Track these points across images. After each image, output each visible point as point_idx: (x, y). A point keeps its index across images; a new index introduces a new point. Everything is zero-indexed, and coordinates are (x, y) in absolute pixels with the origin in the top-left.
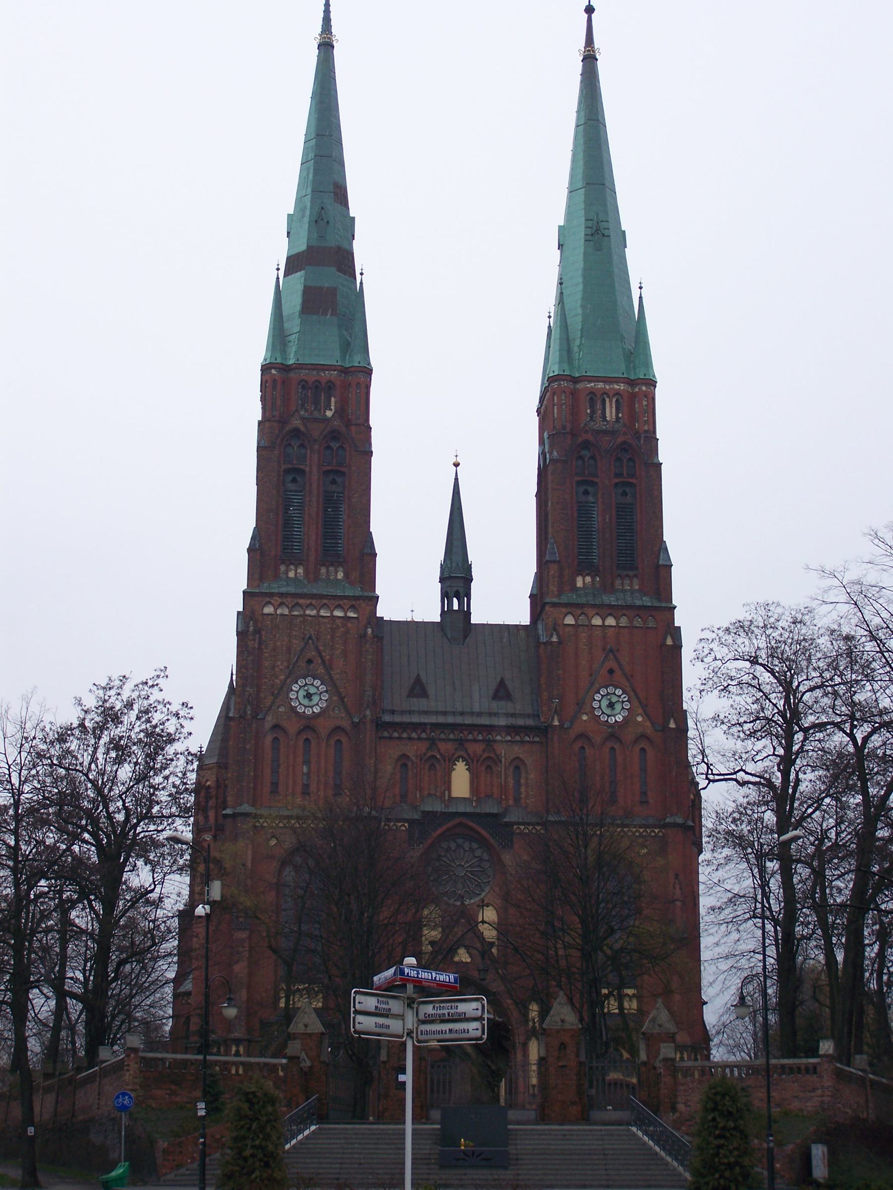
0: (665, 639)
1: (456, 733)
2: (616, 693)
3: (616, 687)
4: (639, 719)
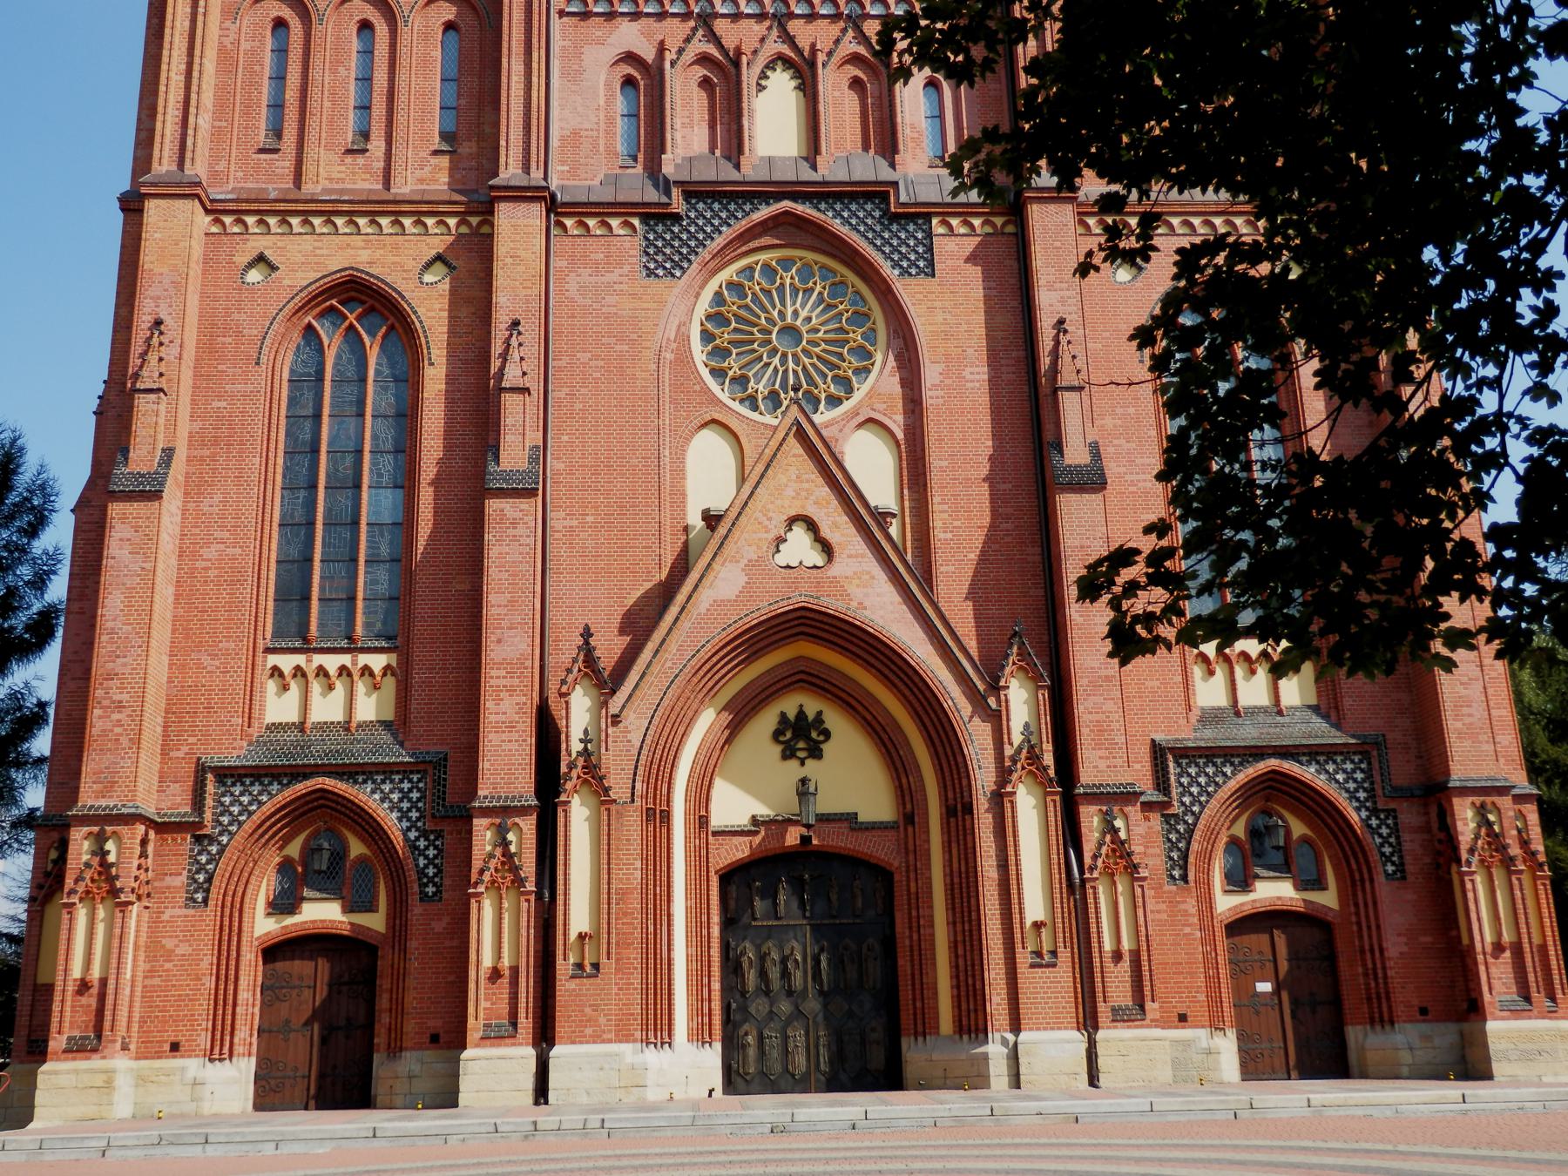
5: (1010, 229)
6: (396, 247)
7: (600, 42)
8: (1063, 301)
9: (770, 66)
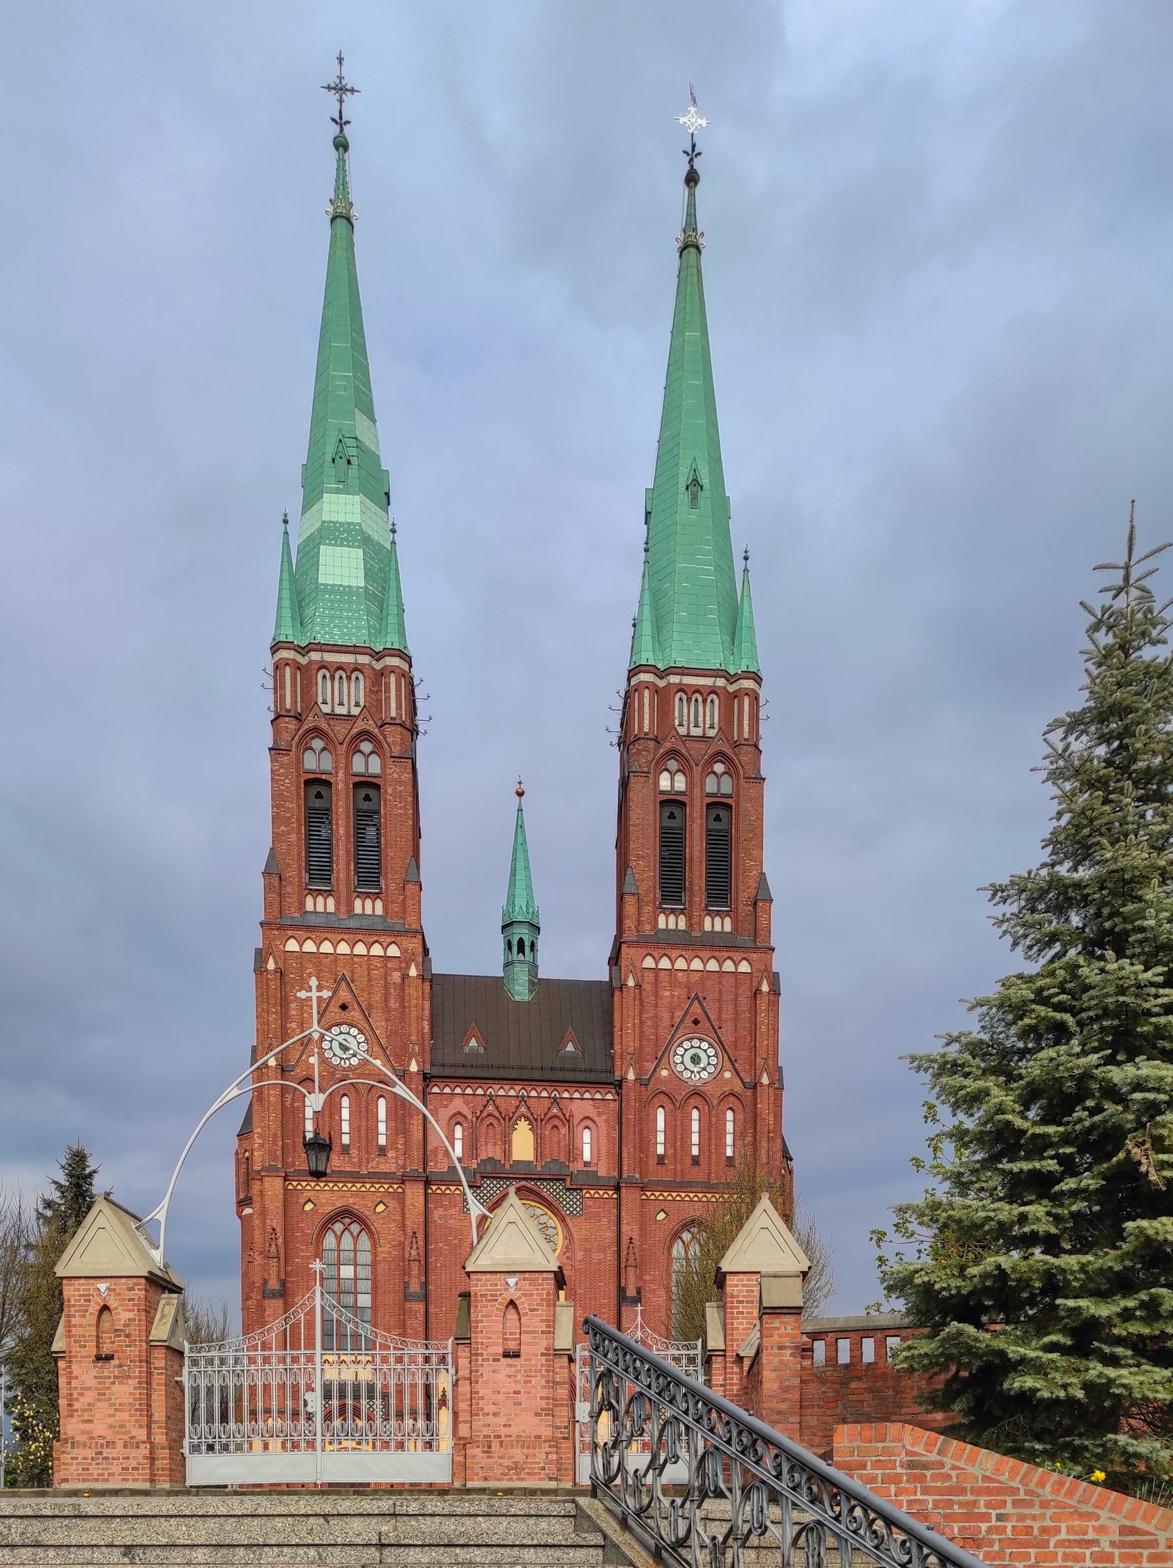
0: (760, 984)
1: (518, 1088)
2: (702, 1046)
3: (702, 1040)
4: (727, 1075)
5: (615, 1196)
6: (363, 1197)
7: (446, 1106)
8: (632, 1230)
9: (519, 1118)
